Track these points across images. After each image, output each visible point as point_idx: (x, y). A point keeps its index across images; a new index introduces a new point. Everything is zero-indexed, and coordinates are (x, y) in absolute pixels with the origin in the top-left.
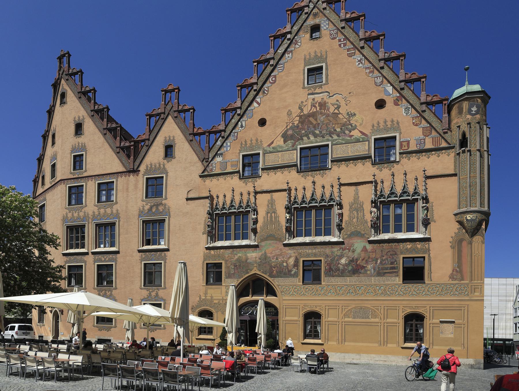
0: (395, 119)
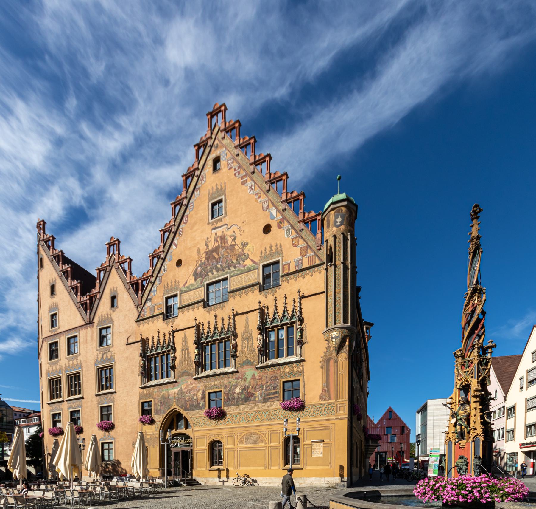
0: (278, 243)
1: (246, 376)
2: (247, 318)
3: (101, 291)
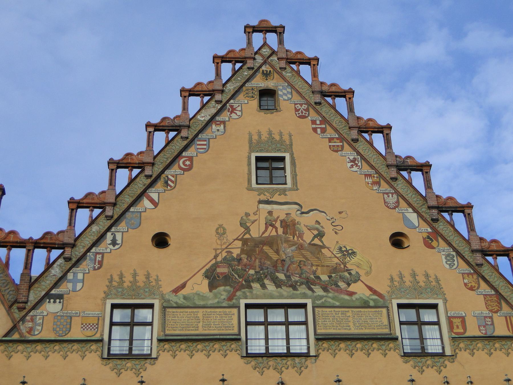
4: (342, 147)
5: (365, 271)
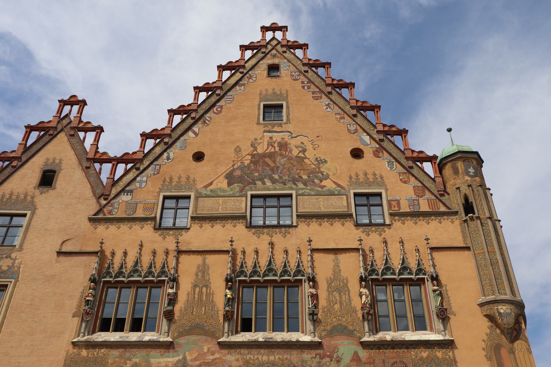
1: (340, 354)
2: (337, 259)
3: (24, 159)
4: (321, 97)
5: (332, 173)
